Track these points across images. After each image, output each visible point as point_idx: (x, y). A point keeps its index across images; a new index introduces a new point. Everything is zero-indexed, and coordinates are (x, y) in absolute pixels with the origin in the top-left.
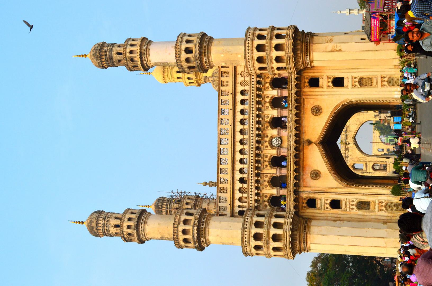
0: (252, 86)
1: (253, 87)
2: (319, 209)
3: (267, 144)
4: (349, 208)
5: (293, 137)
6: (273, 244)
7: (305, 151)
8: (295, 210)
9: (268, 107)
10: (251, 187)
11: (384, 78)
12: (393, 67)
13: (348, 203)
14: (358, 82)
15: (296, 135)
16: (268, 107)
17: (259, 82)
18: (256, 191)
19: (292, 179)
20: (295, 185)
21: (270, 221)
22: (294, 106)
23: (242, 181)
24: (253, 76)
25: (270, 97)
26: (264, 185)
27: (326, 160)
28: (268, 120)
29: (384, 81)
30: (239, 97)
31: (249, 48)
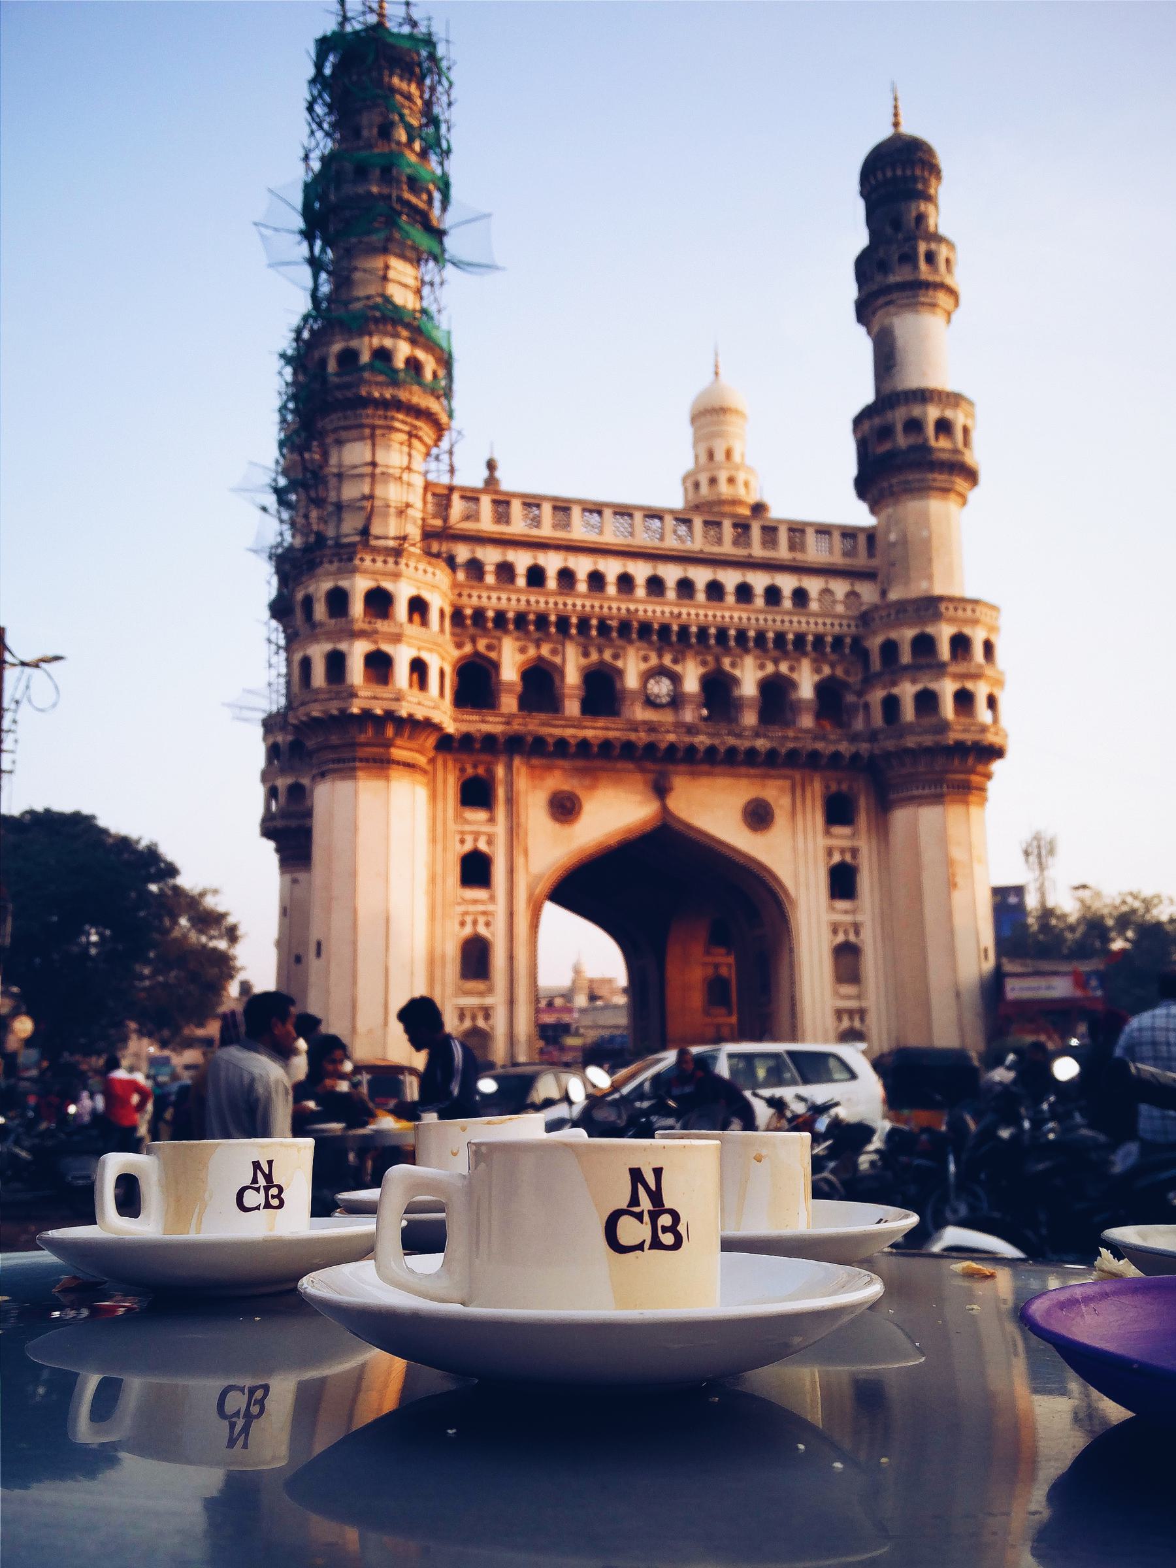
0: (828, 621)
1: (824, 624)
3: (654, 661)
4: (466, 913)
5: (687, 739)
6: (357, 652)
7: (638, 777)
11: (862, 1020)
13: (481, 908)
15: (691, 749)
16: (762, 667)
17: (838, 641)
18: (511, 615)
19: (558, 732)
21: (430, 650)
23: (536, 576)
24: (857, 626)
25: (795, 676)
27: (612, 841)
28: (726, 662)
31: (960, 613)
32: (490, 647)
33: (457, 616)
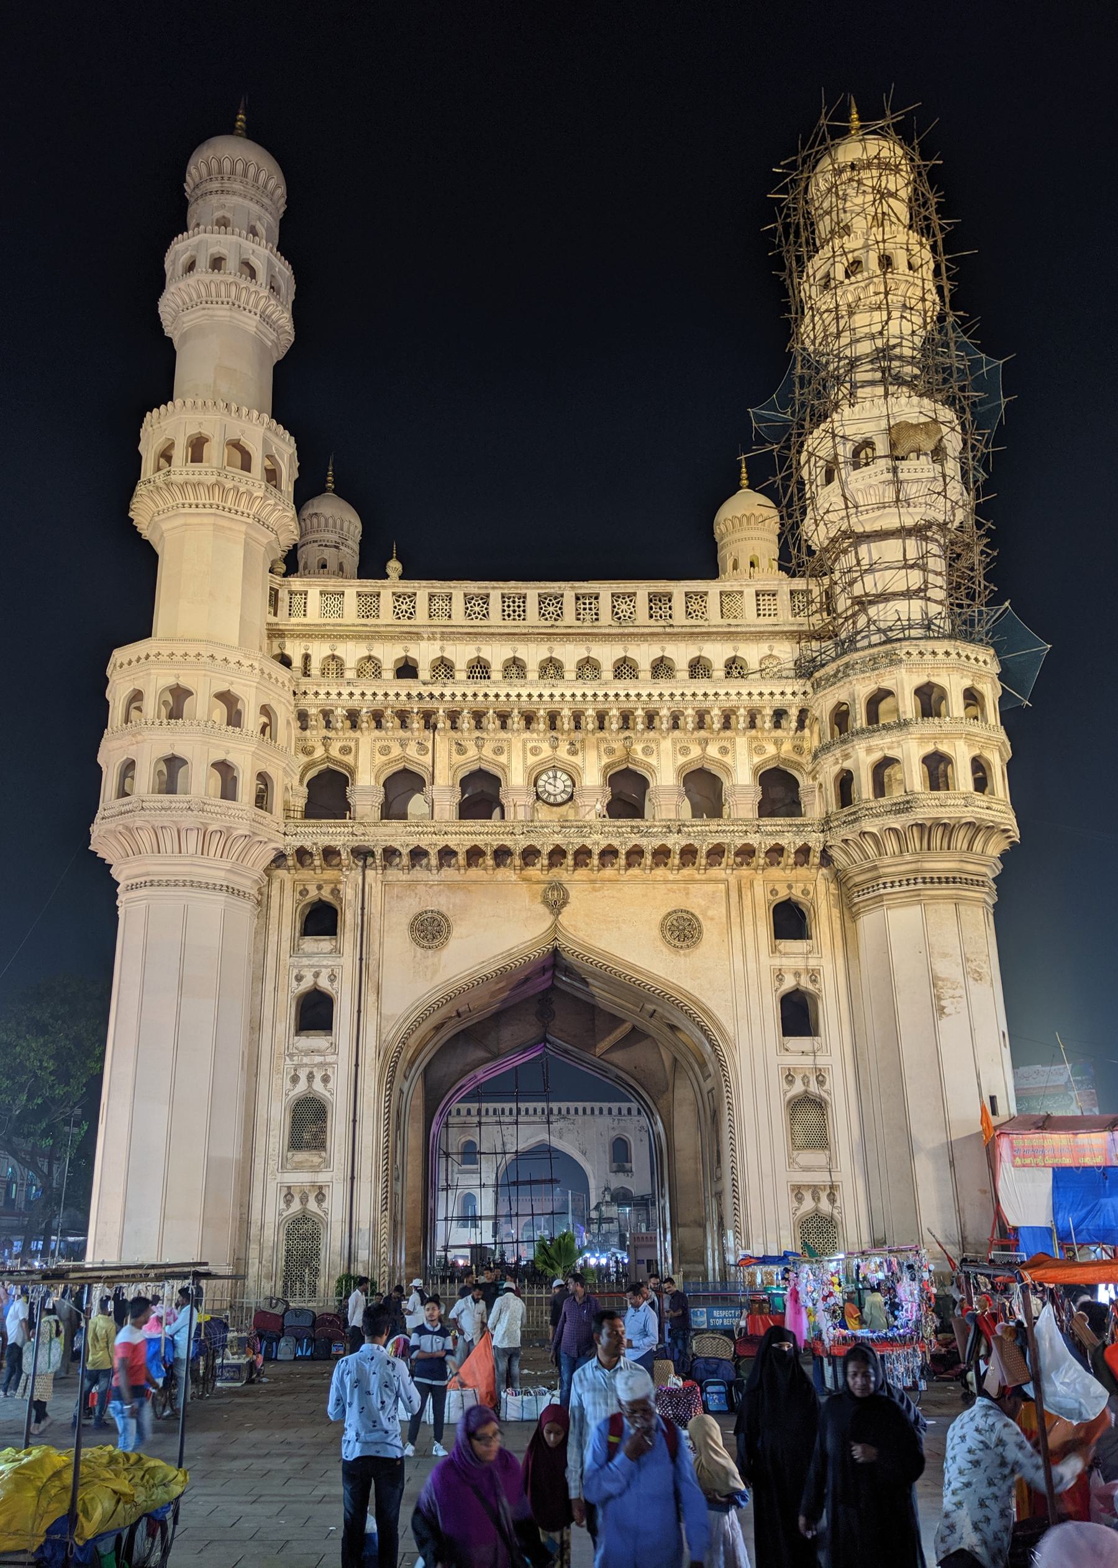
2: (295, 949)
8: (289, 851)
9: (685, 751)
10: (380, 693)
11: (832, 1199)
12: (879, 1236)
13: (318, 1059)
14: (806, 1092)
16: (685, 751)
17: (779, 715)
20: (390, 853)
22: (697, 844)
25: (728, 759)
26: (391, 744)
29: (816, 1198)
30: (717, 653)
32: (345, 750)
33: (303, 717)
